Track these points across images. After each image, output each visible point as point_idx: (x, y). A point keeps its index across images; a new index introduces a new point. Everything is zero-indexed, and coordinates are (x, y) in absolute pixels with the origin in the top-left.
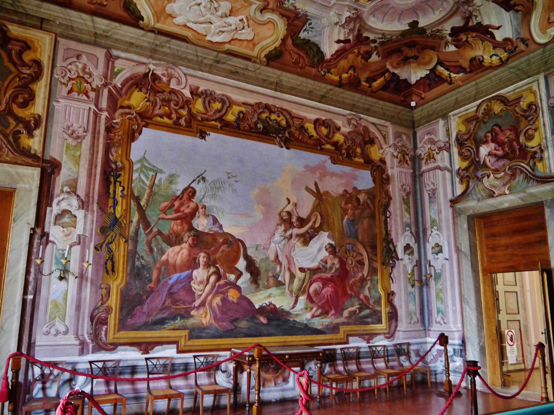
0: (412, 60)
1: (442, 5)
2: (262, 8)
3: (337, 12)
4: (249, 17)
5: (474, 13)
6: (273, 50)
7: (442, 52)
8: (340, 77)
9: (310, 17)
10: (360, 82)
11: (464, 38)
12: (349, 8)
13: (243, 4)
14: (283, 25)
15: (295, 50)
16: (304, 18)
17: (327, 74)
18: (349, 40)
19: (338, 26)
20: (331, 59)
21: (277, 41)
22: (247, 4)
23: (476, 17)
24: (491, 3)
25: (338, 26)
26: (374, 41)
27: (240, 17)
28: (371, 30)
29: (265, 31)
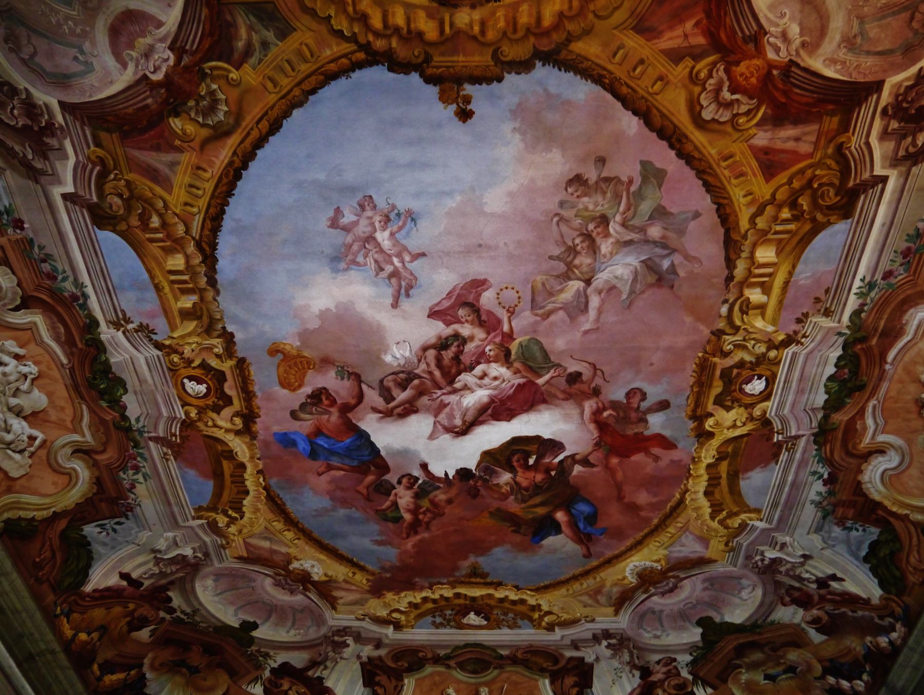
0: (184, 670)
1: (309, 628)
2: (84, 448)
3: (177, 539)
4: (48, 444)
5: (328, 663)
6: (26, 519)
7: (240, 687)
8: (75, 635)
9: (136, 517)
10: (92, 662)
11: (286, 686)
12: (200, 547)
13: (64, 421)
14: (79, 495)
15: (56, 542)
16: (123, 509)
17: (62, 617)
18: (142, 584)
19: (153, 555)
20: (88, 595)
21: (45, 509)
22: (70, 425)
23: (326, 668)
24: (358, 663)
25: (153, 555)
26: (171, 611)
27: (35, 433)
28: (189, 594)
29: (47, 482)
